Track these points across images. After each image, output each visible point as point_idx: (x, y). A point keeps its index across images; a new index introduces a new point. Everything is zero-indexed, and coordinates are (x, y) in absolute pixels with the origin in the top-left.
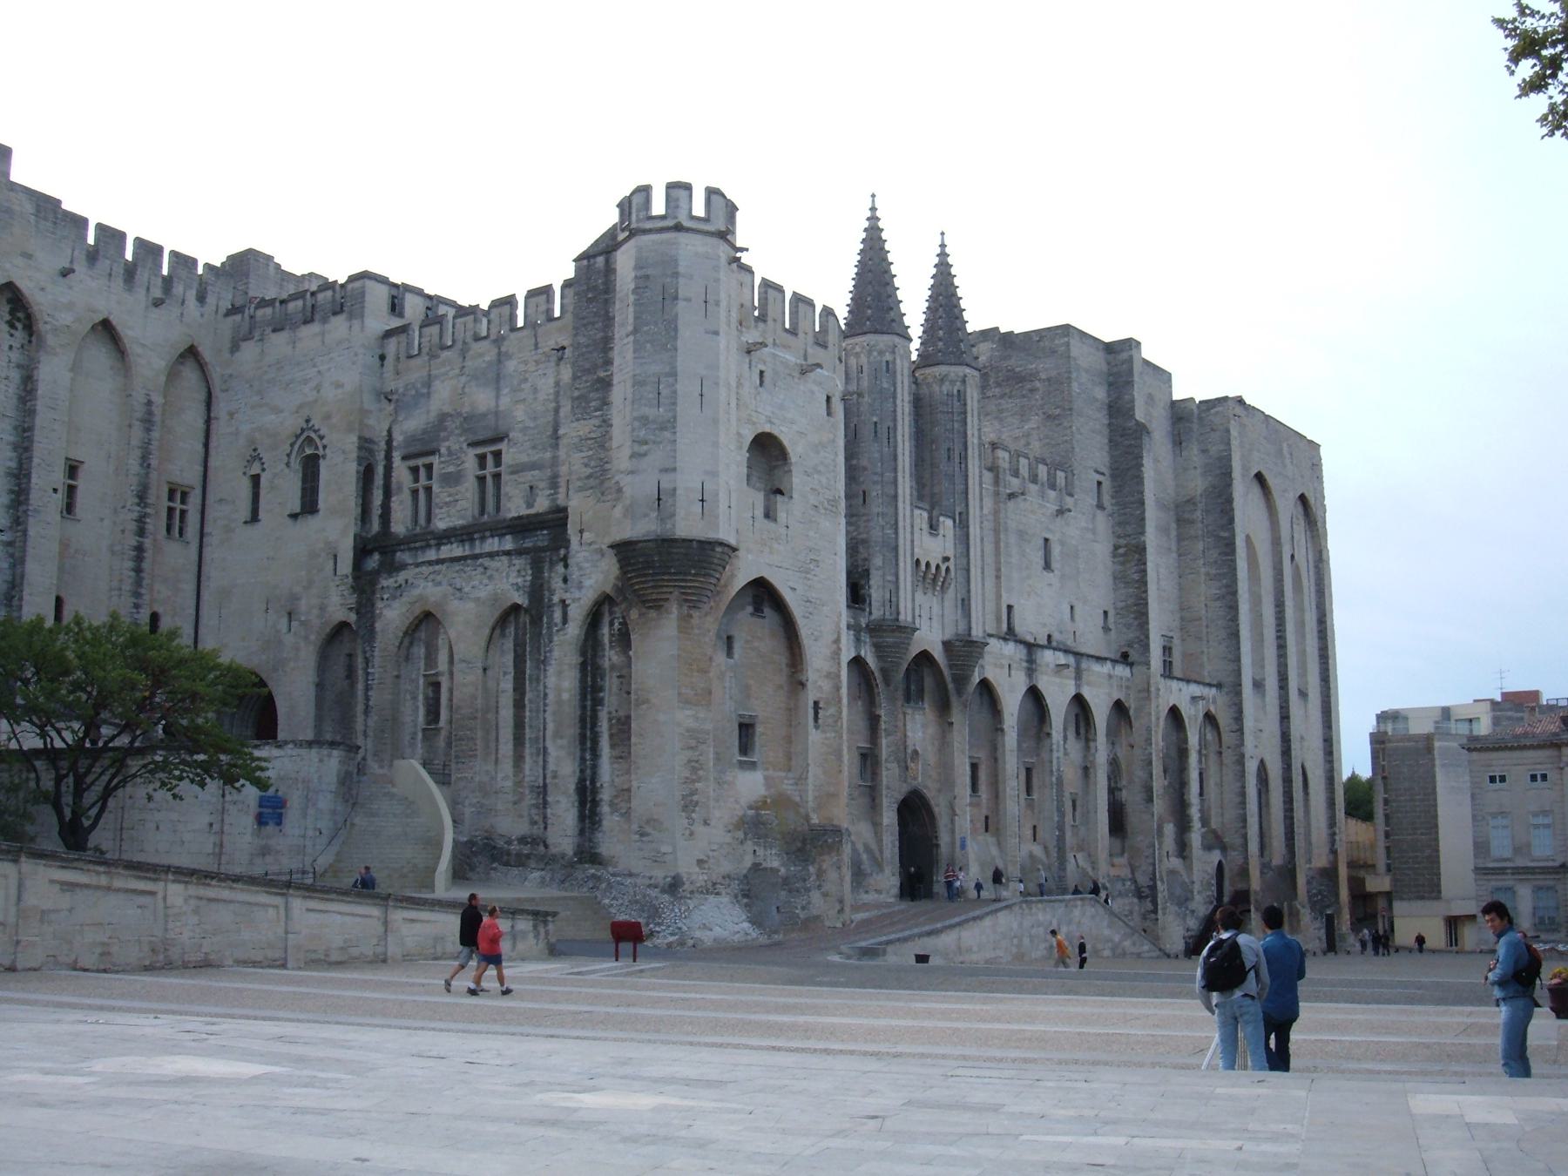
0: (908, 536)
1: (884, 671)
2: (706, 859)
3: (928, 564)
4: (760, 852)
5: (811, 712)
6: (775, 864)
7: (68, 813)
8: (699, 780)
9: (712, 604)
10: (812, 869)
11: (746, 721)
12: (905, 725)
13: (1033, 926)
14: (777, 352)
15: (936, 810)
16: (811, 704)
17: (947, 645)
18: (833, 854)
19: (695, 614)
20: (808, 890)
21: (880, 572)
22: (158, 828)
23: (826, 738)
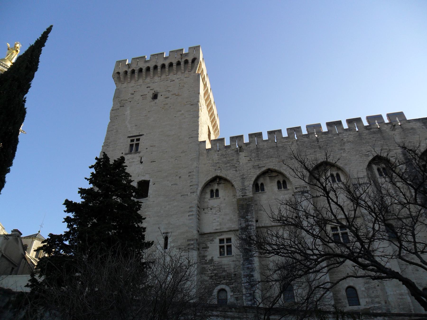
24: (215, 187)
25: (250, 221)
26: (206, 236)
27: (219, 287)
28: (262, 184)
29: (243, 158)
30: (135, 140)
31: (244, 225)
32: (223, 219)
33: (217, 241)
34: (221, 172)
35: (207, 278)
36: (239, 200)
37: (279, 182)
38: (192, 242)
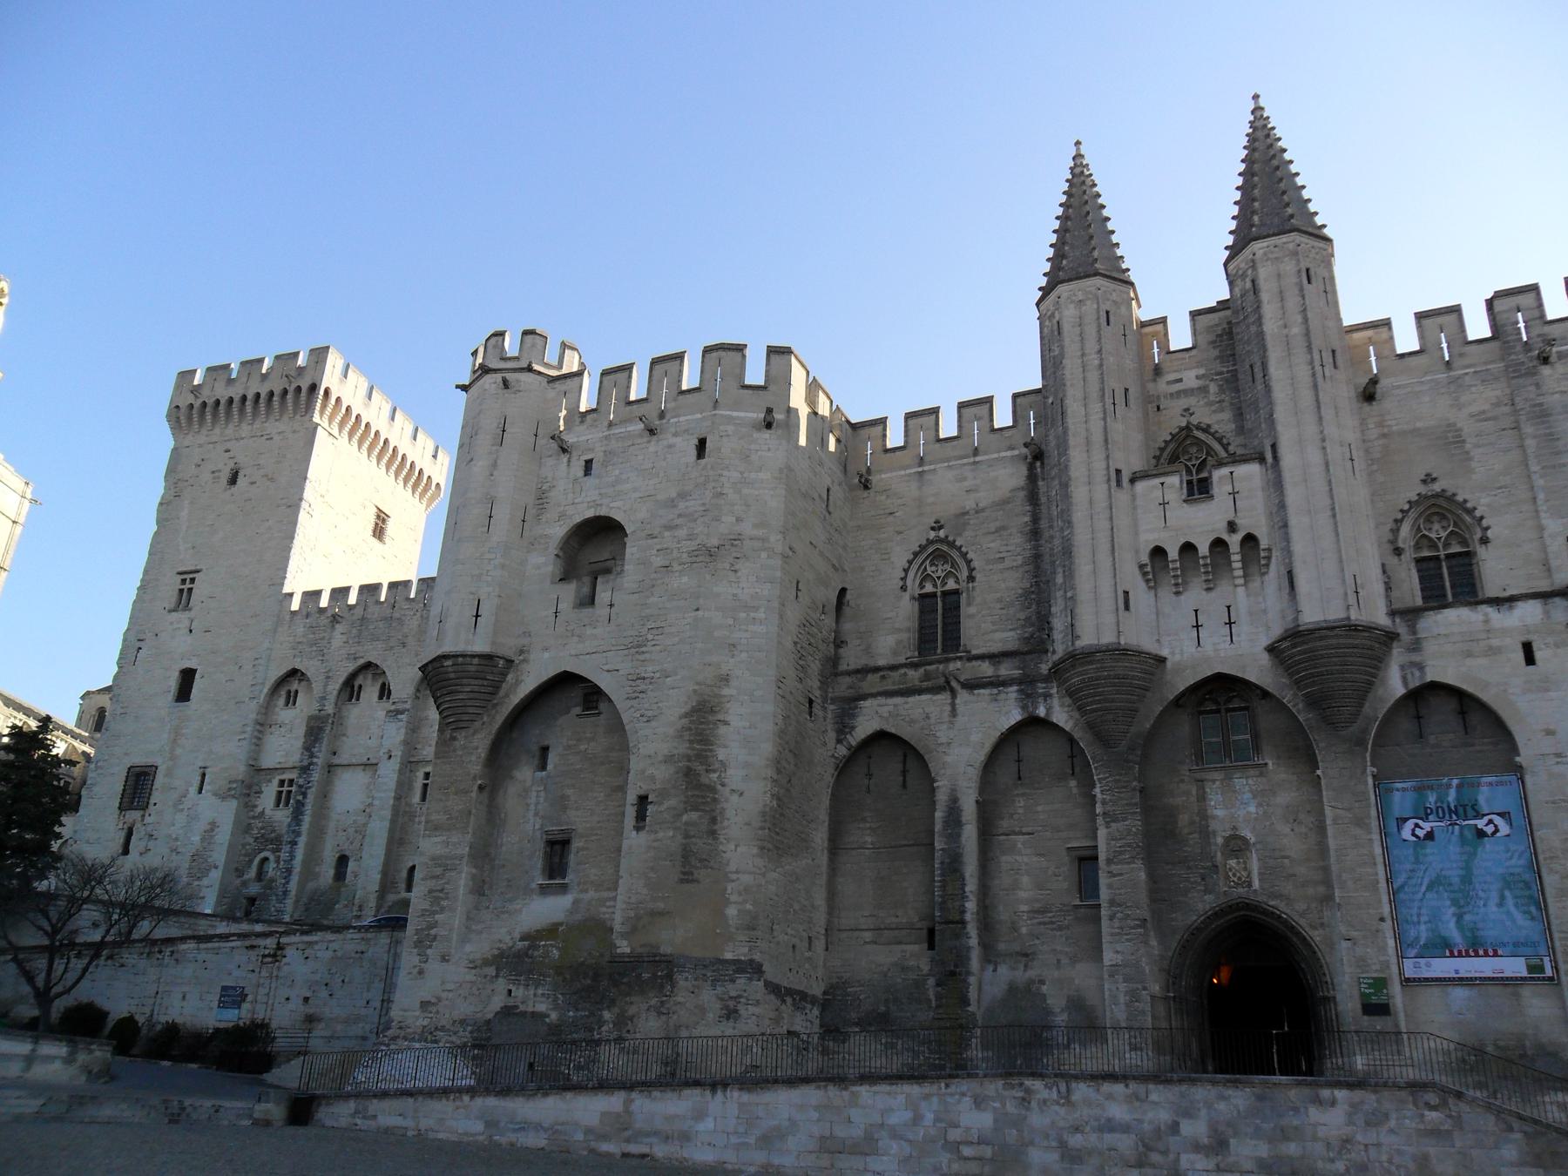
0: (1103, 524)
1: (1091, 726)
2: (433, 1000)
3: (1188, 548)
4: (519, 992)
5: (630, 812)
6: (542, 1007)
7: (40, 981)
8: (442, 910)
9: (485, 719)
10: (607, 1015)
11: (559, 837)
12: (1202, 798)
13: (1077, 1129)
14: (612, 432)
15: (1316, 936)
16: (631, 798)
17: (1271, 649)
18: (651, 995)
19: (461, 735)
20: (598, 1043)
21: (1061, 592)
22: (184, 998)
23: (654, 841)
24: (295, 686)
25: (316, 757)
26: (263, 773)
27: (263, 855)
28: (360, 687)
29: (338, 637)
30: (188, 581)
31: (305, 763)
32: (292, 746)
33: (276, 782)
34: (301, 661)
35: (251, 840)
36: (311, 718)
37: (384, 685)
38: (234, 786)
